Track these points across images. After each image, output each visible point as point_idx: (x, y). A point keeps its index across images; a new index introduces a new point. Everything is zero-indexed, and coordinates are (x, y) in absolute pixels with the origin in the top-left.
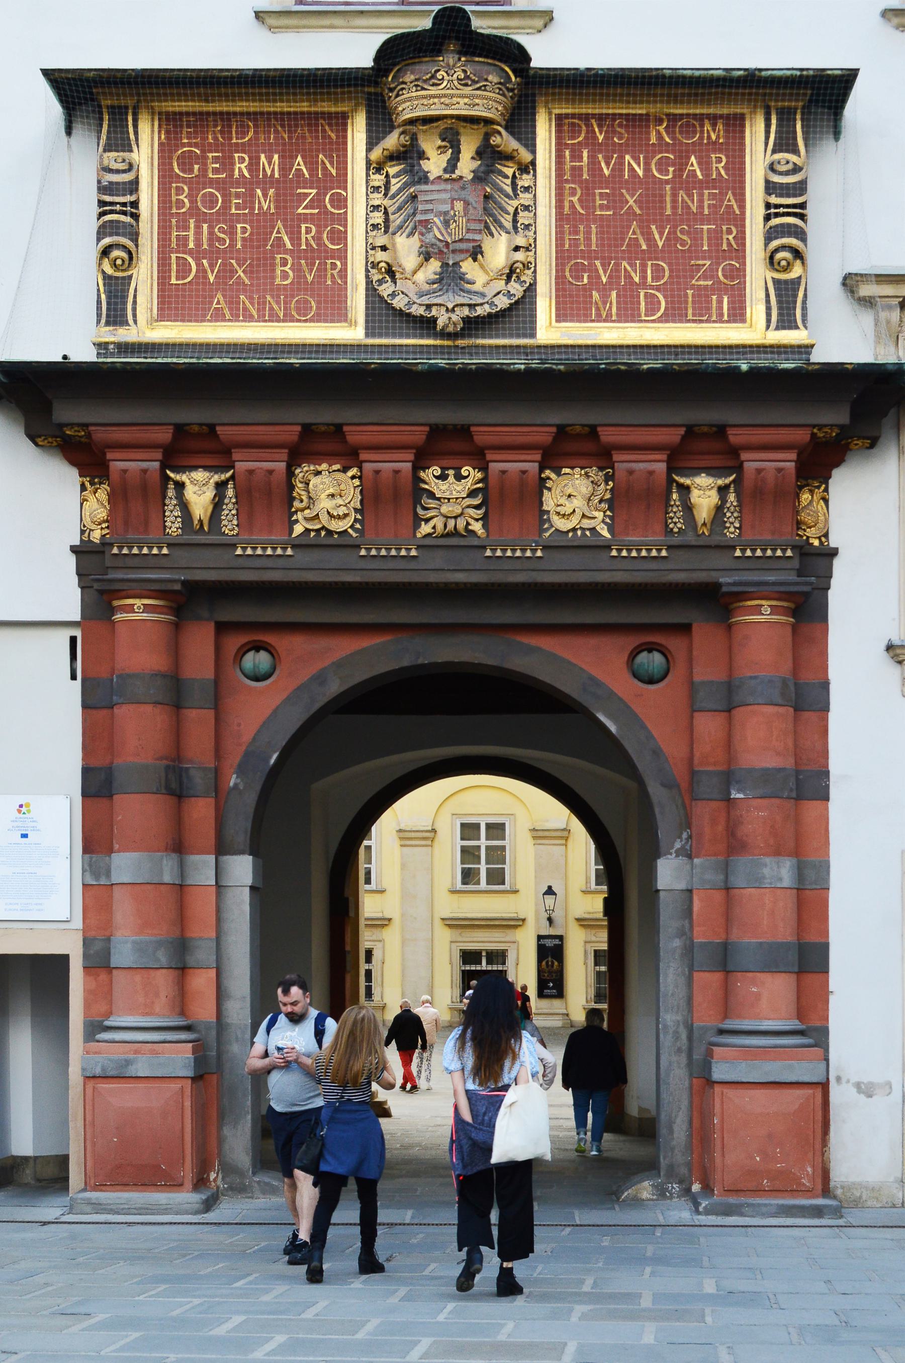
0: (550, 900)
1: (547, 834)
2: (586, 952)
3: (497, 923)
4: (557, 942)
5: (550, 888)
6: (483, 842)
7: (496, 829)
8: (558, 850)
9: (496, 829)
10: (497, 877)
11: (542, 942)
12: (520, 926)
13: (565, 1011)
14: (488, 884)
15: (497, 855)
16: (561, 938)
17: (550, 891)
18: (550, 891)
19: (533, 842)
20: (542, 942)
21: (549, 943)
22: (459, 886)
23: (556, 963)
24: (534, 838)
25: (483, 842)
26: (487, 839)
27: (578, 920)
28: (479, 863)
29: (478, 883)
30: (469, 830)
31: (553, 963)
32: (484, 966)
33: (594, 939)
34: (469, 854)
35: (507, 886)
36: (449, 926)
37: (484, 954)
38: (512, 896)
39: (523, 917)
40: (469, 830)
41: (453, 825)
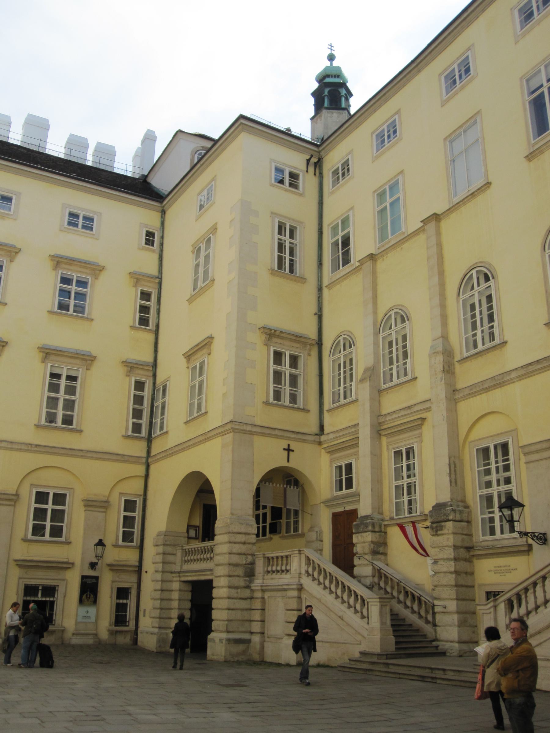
0: (100, 548)
1: (94, 503)
2: (112, 588)
3: (55, 565)
4: (94, 581)
5: (101, 541)
6: (50, 507)
7: (60, 499)
8: (101, 516)
9: (60, 499)
10: (57, 532)
11: (85, 580)
12: (69, 568)
13: (94, 632)
14: (50, 536)
15: (58, 515)
16: (97, 578)
17: (100, 543)
18: (100, 543)
19: (84, 509)
20: (85, 580)
21: (89, 581)
22: (30, 536)
23: (92, 596)
24: (85, 506)
25: (50, 507)
26: (53, 504)
27: (109, 565)
28: (45, 521)
29: (43, 535)
30: (41, 497)
31: (90, 595)
32: (40, 597)
33: (117, 579)
34: (40, 514)
35: (63, 539)
36: (19, 566)
37: (40, 588)
38: (66, 546)
39: (72, 562)
40: (41, 497)
41: (30, 492)
